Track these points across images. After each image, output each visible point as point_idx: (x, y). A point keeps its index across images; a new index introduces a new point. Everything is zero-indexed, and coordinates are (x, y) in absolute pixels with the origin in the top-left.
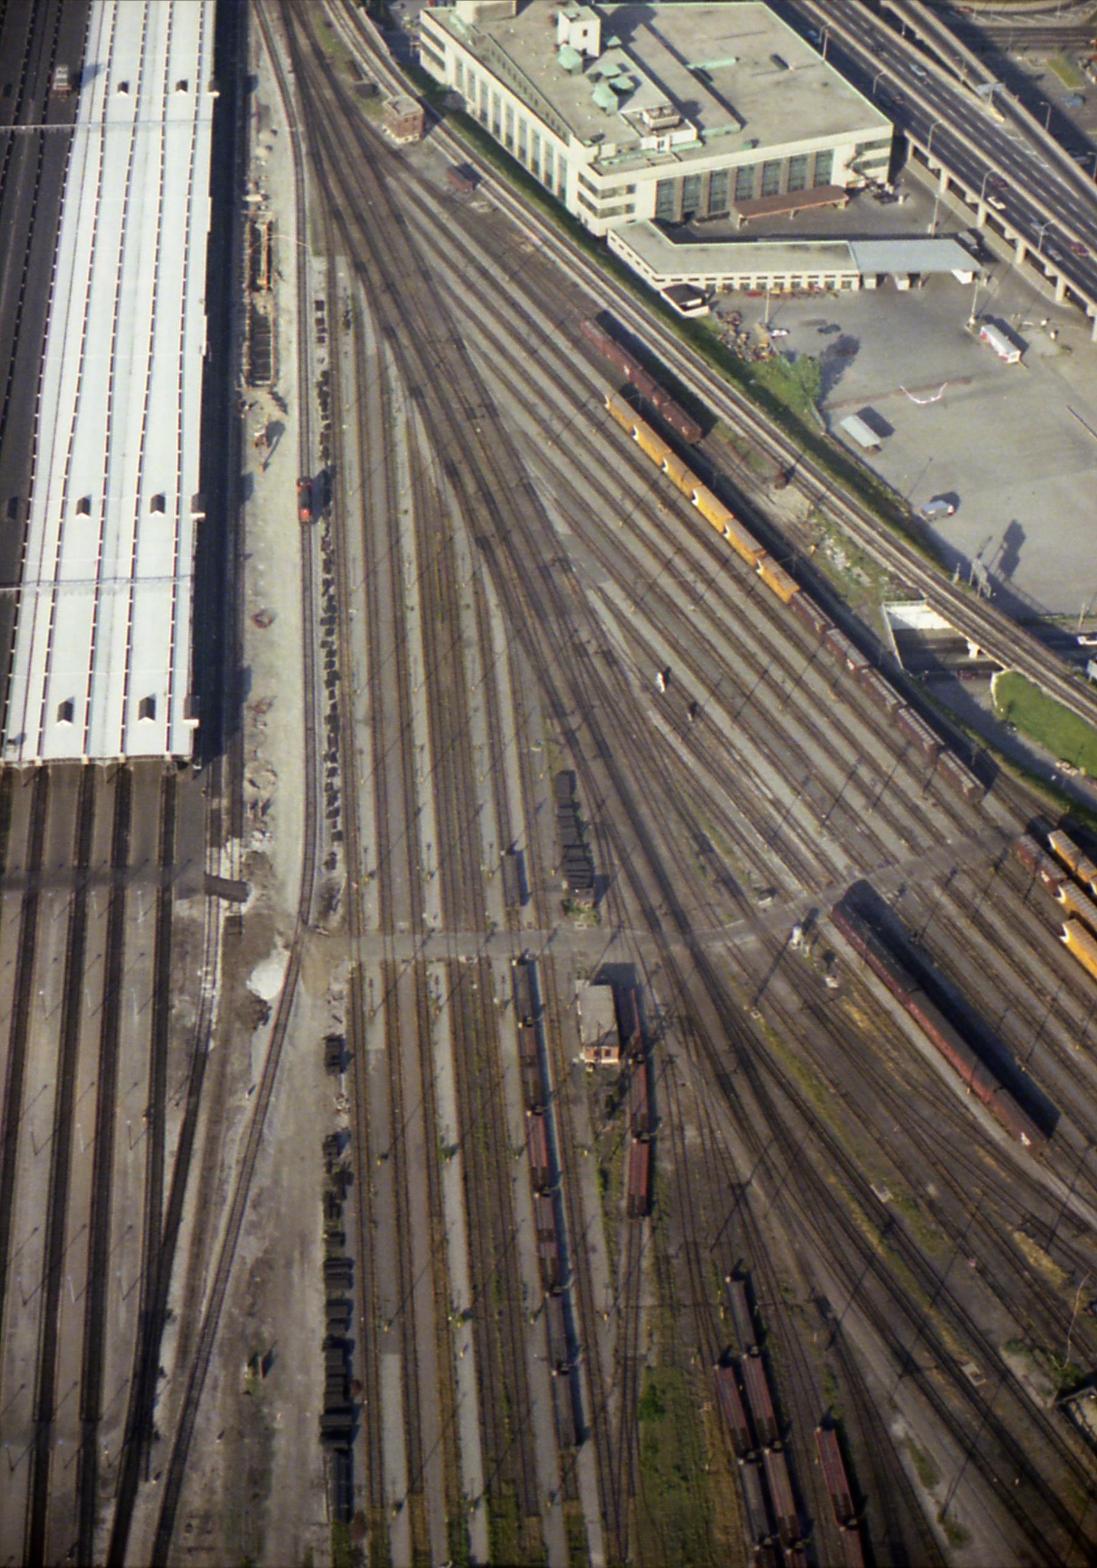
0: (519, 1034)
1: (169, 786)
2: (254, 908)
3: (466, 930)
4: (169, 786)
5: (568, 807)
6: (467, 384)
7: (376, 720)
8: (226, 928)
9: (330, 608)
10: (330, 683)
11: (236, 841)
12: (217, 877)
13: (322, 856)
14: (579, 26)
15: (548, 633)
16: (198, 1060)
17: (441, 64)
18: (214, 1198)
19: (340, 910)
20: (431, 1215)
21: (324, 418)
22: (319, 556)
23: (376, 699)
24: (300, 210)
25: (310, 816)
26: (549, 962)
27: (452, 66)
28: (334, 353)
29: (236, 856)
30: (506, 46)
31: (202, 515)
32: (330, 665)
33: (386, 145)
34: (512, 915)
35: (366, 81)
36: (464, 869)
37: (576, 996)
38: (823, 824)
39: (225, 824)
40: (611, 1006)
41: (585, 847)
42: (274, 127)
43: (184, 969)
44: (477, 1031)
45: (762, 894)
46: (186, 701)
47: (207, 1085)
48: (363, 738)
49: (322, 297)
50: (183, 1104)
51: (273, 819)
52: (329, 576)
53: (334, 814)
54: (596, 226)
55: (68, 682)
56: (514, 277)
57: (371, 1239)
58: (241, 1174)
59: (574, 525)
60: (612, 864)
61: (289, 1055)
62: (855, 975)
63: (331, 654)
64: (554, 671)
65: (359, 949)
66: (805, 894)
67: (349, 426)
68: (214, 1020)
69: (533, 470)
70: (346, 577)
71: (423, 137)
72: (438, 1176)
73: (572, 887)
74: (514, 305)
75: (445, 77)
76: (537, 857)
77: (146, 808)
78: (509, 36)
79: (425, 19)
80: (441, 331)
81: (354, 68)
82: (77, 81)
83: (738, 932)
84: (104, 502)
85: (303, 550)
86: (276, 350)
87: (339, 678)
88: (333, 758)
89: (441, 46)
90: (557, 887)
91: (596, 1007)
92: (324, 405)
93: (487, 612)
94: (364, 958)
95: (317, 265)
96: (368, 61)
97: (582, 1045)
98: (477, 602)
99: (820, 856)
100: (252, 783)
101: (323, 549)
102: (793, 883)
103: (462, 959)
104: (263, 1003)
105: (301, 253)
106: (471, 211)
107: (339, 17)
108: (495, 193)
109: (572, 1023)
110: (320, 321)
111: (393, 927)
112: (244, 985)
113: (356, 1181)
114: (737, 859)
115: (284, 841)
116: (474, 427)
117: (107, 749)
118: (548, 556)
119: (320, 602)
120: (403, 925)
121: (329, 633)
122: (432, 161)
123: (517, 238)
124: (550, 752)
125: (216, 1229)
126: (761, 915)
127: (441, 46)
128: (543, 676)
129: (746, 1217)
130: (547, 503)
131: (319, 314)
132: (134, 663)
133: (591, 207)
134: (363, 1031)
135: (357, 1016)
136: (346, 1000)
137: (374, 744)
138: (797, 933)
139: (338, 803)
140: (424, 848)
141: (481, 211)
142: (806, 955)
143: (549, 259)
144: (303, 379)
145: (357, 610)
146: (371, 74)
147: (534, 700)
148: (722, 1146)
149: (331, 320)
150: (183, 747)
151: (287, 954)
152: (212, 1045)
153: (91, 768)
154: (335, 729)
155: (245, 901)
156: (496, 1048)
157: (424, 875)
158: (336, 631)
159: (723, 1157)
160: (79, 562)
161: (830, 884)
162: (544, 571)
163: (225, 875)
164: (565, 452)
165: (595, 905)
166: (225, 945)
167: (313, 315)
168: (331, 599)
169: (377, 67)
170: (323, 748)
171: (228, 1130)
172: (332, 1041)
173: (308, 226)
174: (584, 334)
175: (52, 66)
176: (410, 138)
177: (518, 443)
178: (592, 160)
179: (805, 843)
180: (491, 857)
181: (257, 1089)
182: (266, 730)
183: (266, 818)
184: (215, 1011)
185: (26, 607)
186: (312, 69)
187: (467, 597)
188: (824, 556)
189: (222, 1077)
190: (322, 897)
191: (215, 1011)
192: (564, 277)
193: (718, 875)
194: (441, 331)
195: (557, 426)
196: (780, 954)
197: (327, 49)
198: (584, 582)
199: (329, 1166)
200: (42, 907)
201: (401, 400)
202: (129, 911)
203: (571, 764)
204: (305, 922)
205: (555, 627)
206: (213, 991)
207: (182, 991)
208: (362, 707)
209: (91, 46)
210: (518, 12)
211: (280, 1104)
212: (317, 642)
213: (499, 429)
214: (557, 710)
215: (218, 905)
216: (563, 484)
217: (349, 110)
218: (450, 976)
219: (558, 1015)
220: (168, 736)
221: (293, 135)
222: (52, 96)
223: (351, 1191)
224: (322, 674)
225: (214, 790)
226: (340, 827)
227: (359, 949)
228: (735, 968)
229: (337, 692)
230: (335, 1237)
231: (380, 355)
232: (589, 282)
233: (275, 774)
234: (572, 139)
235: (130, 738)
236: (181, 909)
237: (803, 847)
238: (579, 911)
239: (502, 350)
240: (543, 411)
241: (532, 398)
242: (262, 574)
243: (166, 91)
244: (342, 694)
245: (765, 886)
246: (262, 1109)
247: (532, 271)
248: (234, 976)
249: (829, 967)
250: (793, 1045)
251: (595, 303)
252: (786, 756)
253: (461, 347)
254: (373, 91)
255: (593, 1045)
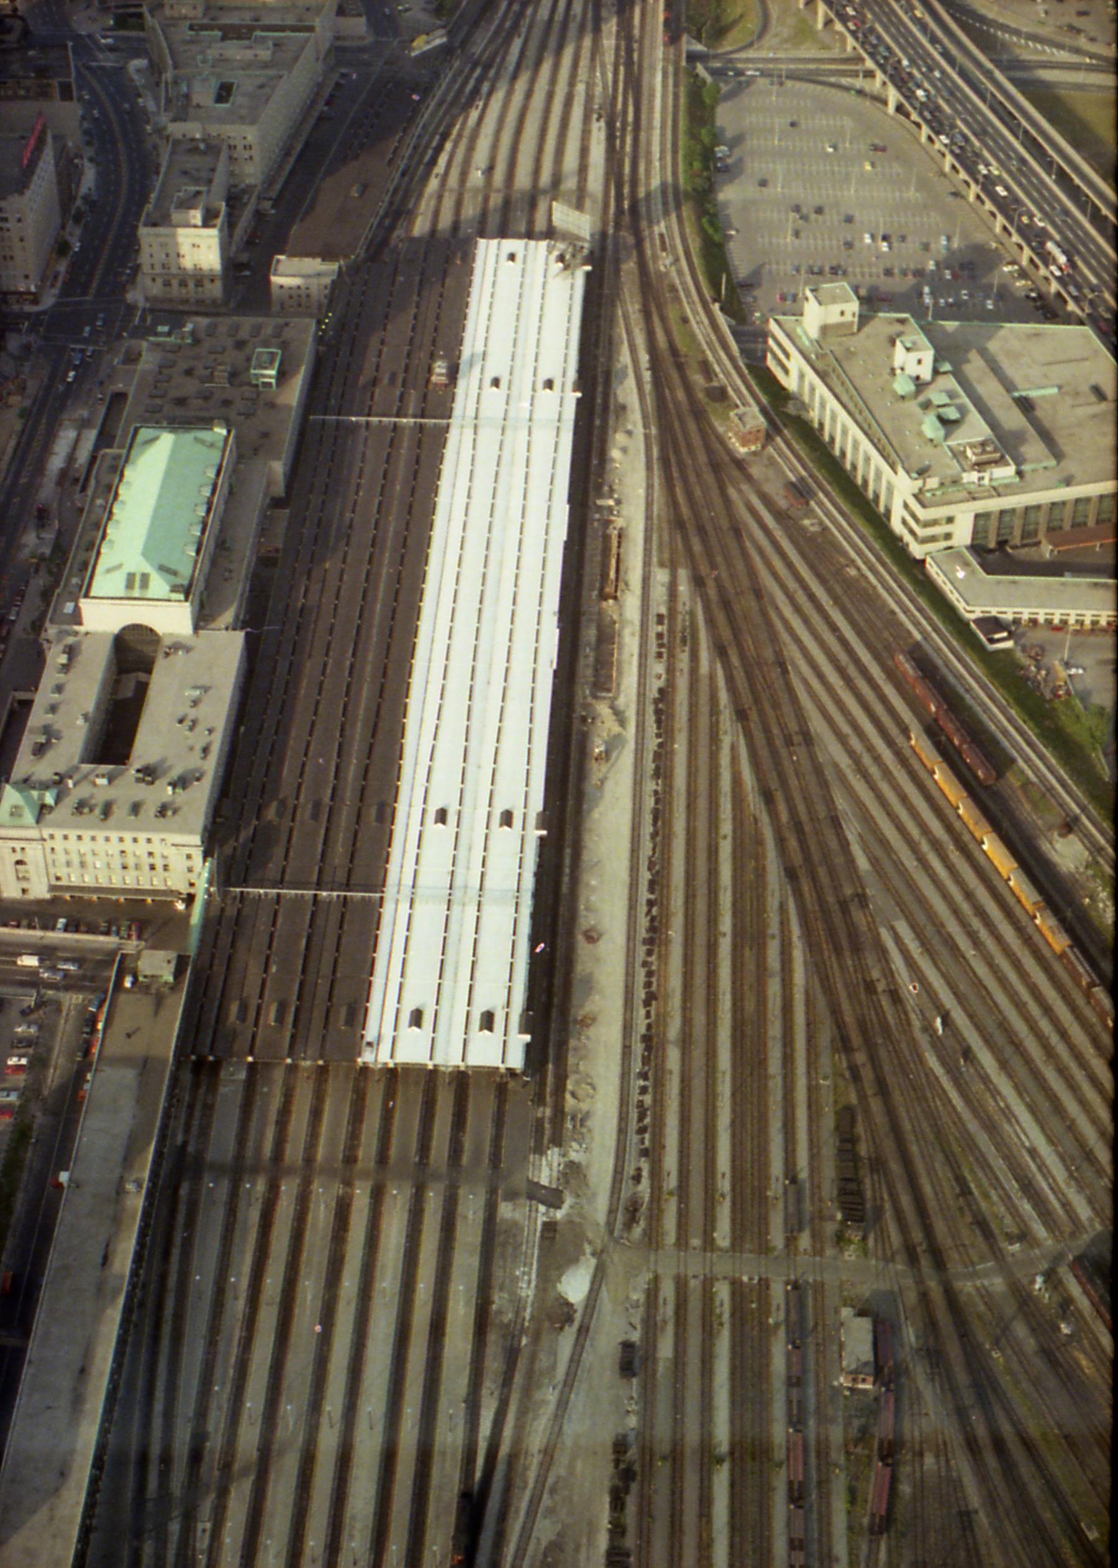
0: (788, 1355)
1: (502, 1090)
2: (568, 1215)
3: (751, 1252)
4: (502, 1090)
5: (847, 1140)
6: (787, 709)
7: (686, 1041)
8: (543, 1231)
9: (652, 929)
10: (647, 1003)
11: (556, 1150)
12: (537, 1184)
13: (629, 1170)
14: (914, 356)
15: (842, 967)
16: (512, 1355)
17: (786, 371)
18: (518, 1482)
19: (642, 1223)
20: (701, 1516)
21: (658, 736)
22: (645, 876)
23: (687, 1021)
24: (648, 517)
25: (622, 1131)
26: (819, 1288)
27: (795, 374)
28: (670, 670)
29: (555, 1164)
30: (845, 364)
31: (544, 832)
32: (648, 985)
33: (729, 452)
34: (791, 1241)
35: (715, 384)
36: (753, 1193)
37: (842, 1324)
38: (1071, 1176)
39: (548, 1133)
40: (869, 1337)
41: (860, 1182)
42: (630, 427)
43: (505, 1268)
44: (752, 1347)
45: (1011, 1239)
46: (521, 1016)
47: (518, 1379)
48: (673, 1056)
49: (663, 610)
50: (496, 1393)
51: (590, 1131)
52: (652, 897)
53: (642, 1131)
54: (917, 550)
55: (420, 993)
56: (836, 600)
57: (649, 1530)
58: (541, 1464)
59: (874, 861)
60: (882, 1199)
61: (588, 1357)
62: (1086, 1322)
63: (650, 974)
64: (846, 1006)
65: (656, 1262)
66: (1050, 1242)
67: (680, 747)
68: (528, 1317)
69: (842, 803)
70: (668, 899)
71: (764, 447)
72: (710, 1480)
73: (845, 1220)
74: (834, 629)
75: (790, 383)
76: (816, 1186)
77: (481, 1109)
78: (850, 354)
79: (773, 326)
80: (768, 654)
81: (706, 369)
82: (453, 373)
83: (986, 1274)
84: (459, 813)
85: (632, 869)
86: (619, 662)
87: (656, 999)
88: (644, 1076)
89: (787, 355)
90: (832, 1218)
91: (857, 1339)
92: (659, 722)
93: (790, 944)
94: (660, 1271)
95: (661, 576)
96: (719, 361)
97: (842, 1370)
98: (782, 932)
99: (1066, 1205)
100: (573, 1095)
101: (649, 869)
102: (1040, 1230)
103: (745, 1279)
104: (570, 1305)
105: (647, 564)
106: (803, 529)
107: (695, 313)
108: (826, 512)
109: (835, 1348)
110: (660, 636)
111: (687, 1243)
112: (555, 1287)
113: (639, 1478)
114: (993, 1204)
115: (598, 1148)
116: (791, 755)
117: (450, 1058)
118: (848, 891)
119: (643, 922)
120: (696, 1242)
121: (649, 953)
122: (771, 473)
123: (842, 560)
124: (836, 1087)
125: (517, 1511)
126: (1010, 1259)
127: (787, 355)
128: (835, 1011)
129: (970, 1541)
130: (851, 837)
131: (660, 628)
132: (477, 974)
133: (912, 532)
134: (655, 1341)
135: (651, 1326)
136: (642, 1309)
137: (683, 1065)
138: (1039, 1280)
139: (647, 1121)
140: (719, 1176)
141: (812, 529)
142: (1046, 1301)
143: (869, 583)
144: (641, 695)
145: (676, 933)
146: (721, 376)
147: (826, 1035)
148: (954, 1474)
149: (670, 637)
150: (516, 1060)
151: (593, 1262)
152: (524, 1341)
153: (435, 1071)
154: (648, 1048)
155: (559, 1207)
156: (768, 1365)
157: (717, 1196)
158: (656, 950)
159: (957, 1484)
160: (434, 874)
161: (1073, 1235)
162: (844, 906)
163: (544, 1181)
164: (873, 788)
165: (864, 1238)
166: (541, 1249)
167: (655, 629)
168: (653, 919)
169: (728, 372)
170: (637, 1066)
171: (534, 1419)
172: (627, 1346)
173: (655, 537)
174: (897, 666)
175: (432, 357)
176: (753, 448)
177: (829, 773)
178: (916, 491)
179: (1054, 1192)
180: (776, 1187)
181: (559, 1387)
182: (590, 1045)
183: (584, 1130)
184: (529, 1310)
185: (387, 911)
186: (669, 364)
187: (774, 928)
188: (1097, 909)
189: (530, 1374)
190: (626, 1209)
191: (529, 1310)
192: (884, 604)
193: (974, 1216)
194: (768, 654)
195: (867, 760)
196: (1024, 1299)
197: (682, 347)
198: (878, 919)
199: (617, 1462)
200: (388, 1201)
201: (728, 723)
202: (460, 1209)
203: (853, 1099)
204: (611, 1232)
205: (850, 963)
206: (527, 1290)
207: (501, 1289)
208: (674, 1029)
209: (468, 336)
210: (859, 330)
211: (578, 1400)
212: (638, 964)
213: (813, 757)
214: (844, 1044)
215: (537, 1211)
216: (866, 818)
217: (699, 414)
218: (733, 1294)
219: (824, 1339)
220: (503, 1049)
221: (647, 437)
222: (431, 387)
223: (634, 1487)
224: (640, 994)
225: (540, 1099)
226: (647, 1143)
227: (656, 1262)
228: (982, 1308)
229: (653, 1013)
230: (617, 1530)
231: (712, 677)
232: (906, 611)
233: (594, 1089)
234: (900, 469)
235: (471, 1047)
236: (505, 1210)
237: (1051, 1197)
238: (850, 1242)
239: (821, 677)
240: (855, 743)
241: (846, 729)
242: (594, 889)
243: (534, 390)
244: (658, 1015)
245: (1014, 1230)
246: (563, 1404)
247: (856, 598)
248: (548, 1276)
249: (1064, 1312)
250: (1026, 1385)
251: (909, 633)
252: (1045, 1106)
253: (785, 672)
254: (720, 395)
255: (851, 1373)
